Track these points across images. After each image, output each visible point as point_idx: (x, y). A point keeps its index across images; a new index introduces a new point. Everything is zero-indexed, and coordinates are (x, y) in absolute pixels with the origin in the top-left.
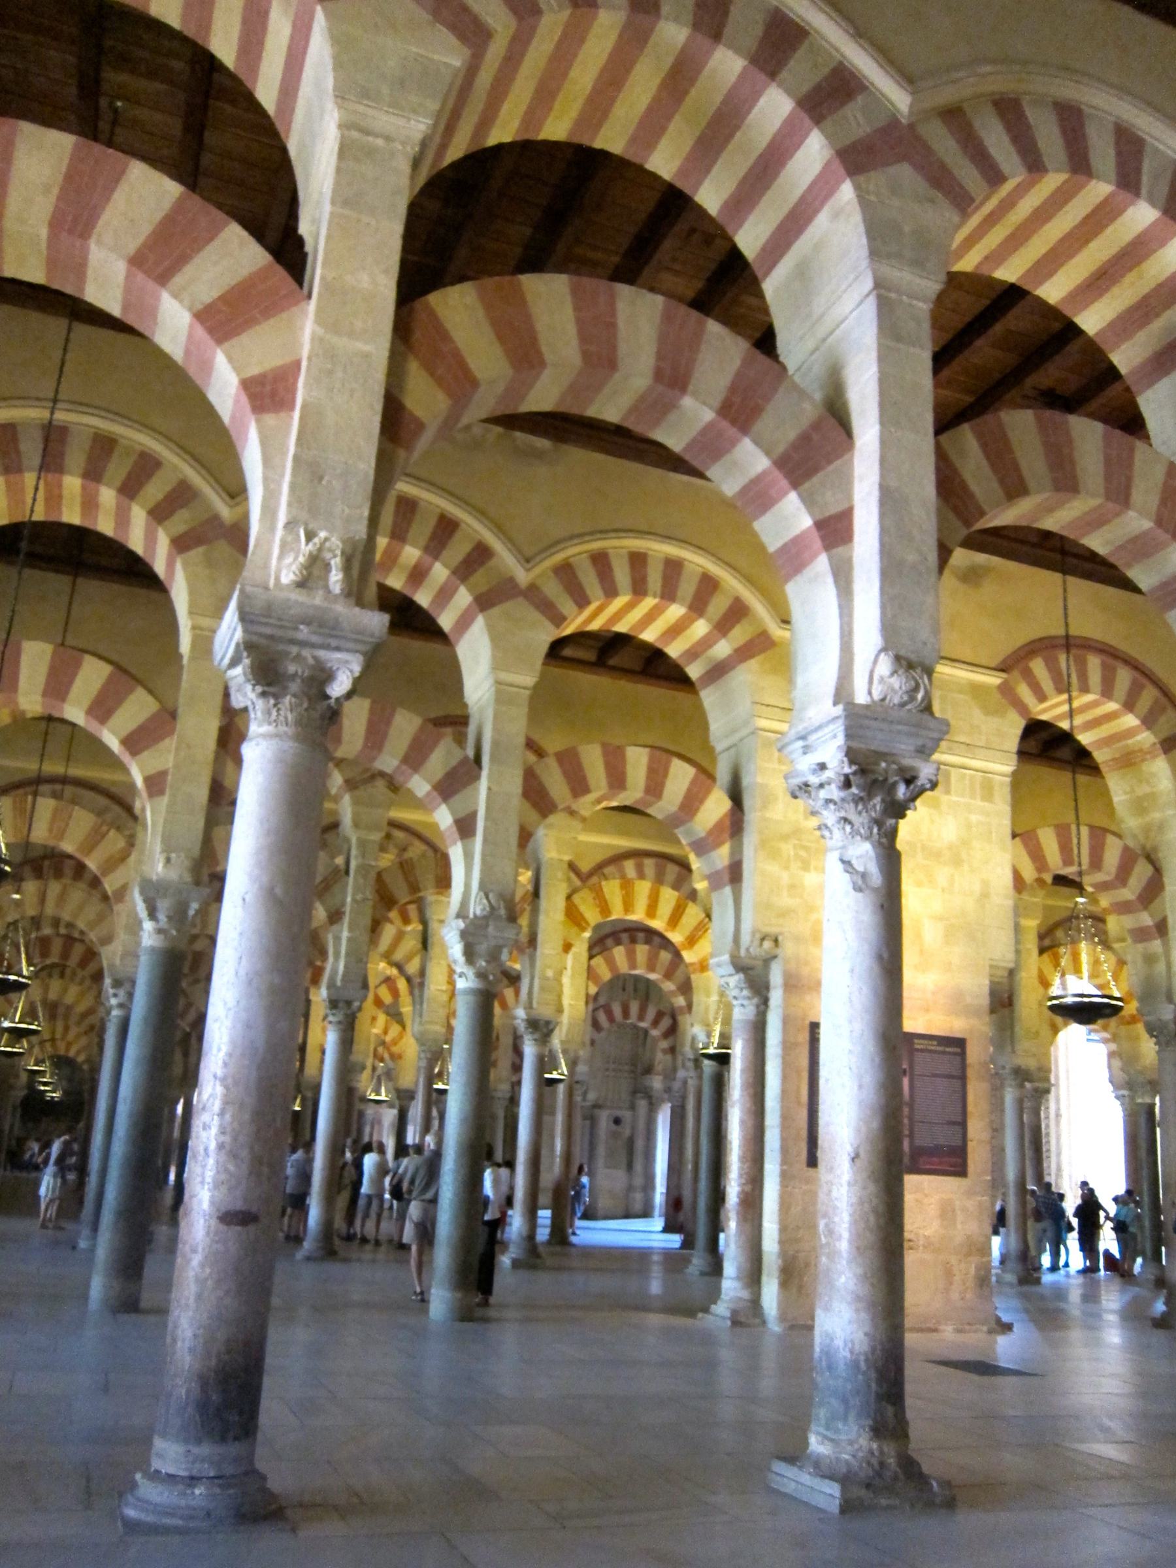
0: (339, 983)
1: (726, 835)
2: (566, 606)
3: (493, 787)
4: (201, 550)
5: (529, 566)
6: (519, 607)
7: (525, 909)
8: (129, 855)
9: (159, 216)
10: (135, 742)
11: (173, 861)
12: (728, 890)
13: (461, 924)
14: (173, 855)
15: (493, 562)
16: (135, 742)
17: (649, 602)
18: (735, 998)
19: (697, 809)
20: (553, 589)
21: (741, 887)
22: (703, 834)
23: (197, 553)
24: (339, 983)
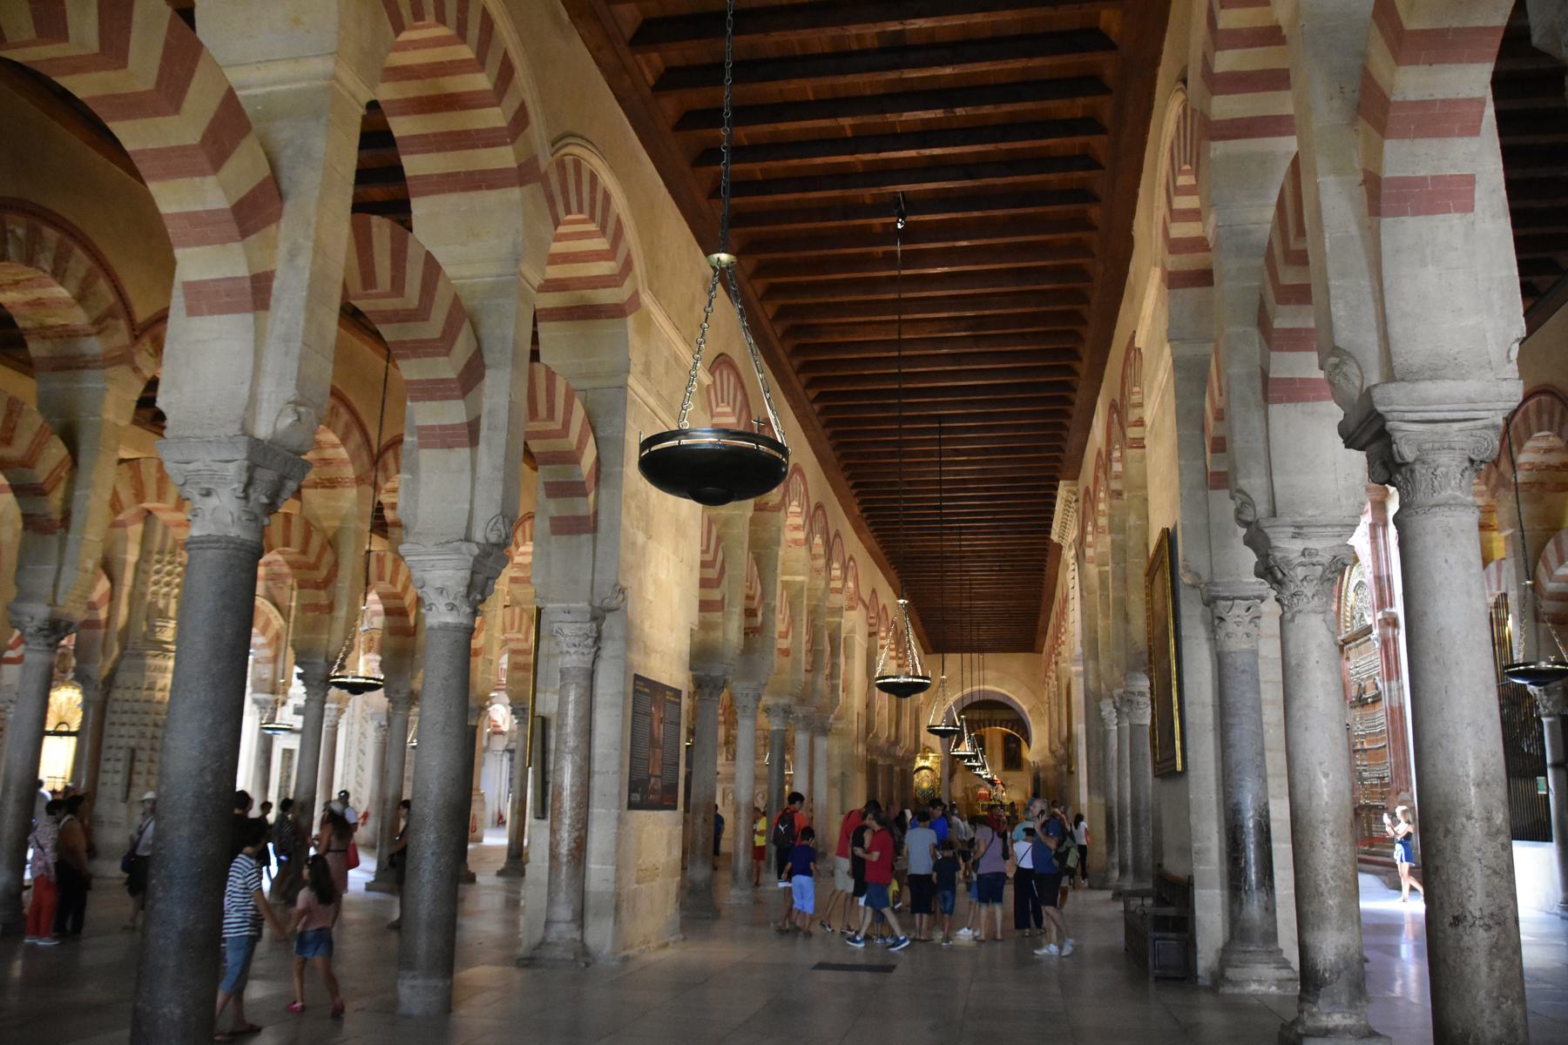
6: (534, 188)
7: (61, 478)
11: (302, 417)
13: (476, 551)
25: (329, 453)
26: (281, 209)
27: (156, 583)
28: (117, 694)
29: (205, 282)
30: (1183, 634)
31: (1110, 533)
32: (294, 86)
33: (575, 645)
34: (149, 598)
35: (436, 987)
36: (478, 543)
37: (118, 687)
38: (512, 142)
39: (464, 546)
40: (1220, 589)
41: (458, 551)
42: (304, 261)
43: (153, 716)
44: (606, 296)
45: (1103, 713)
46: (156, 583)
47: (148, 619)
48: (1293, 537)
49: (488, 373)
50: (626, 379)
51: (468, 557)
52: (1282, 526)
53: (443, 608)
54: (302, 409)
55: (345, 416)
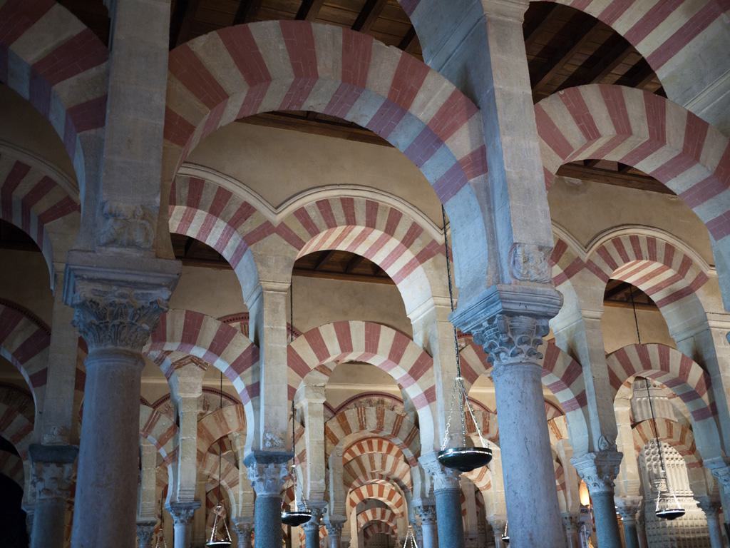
0: (427, 496)
1: (705, 388)
2: (607, 270)
3: (595, 376)
4: (431, 259)
5: (586, 250)
6: (586, 273)
8: (303, 432)
9: (684, 127)
10: (416, 372)
11: (454, 438)
12: (711, 419)
13: (595, 456)
14: (453, 435)
15: (568, 249)
16: (416, 372)
17: (644, 262)
18: (725, 480)
19: (688, 375)
20: (599, 262)
21: (718, 417)
22: (694, 388)
23: (429, 262)
24: (427, 496)
26: (432, 361)
27: (649, 460)
28: (648, 525)
32: (428, 312)
34: (647, 469)
37: (648, 522)
38: (556, 263)
39: (588, 455)
41: (587, 458)
42: (440, 379)
43: (663, 536)
44: (681, 285)
46: (649, 460)
47: (650, 481)
49: (584, 368)
50: (708, 324)
53: (592, 486)
54: (453, 435)
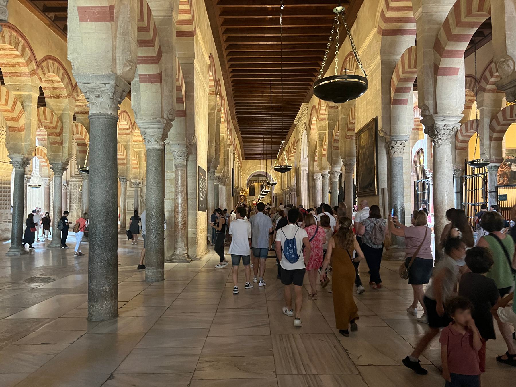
25: (56, 85)
29: (88, 8)
30: (379, 152)
31: (328, 120)
33: (180, 156)
35: (160, 272)
36: (166, 119)
40: (394, 138)
45: (315, 178)
48: (442, 120)
51: (163, 124)
52: (440, 117)
53: (153, 142)
55: (62, 71)
